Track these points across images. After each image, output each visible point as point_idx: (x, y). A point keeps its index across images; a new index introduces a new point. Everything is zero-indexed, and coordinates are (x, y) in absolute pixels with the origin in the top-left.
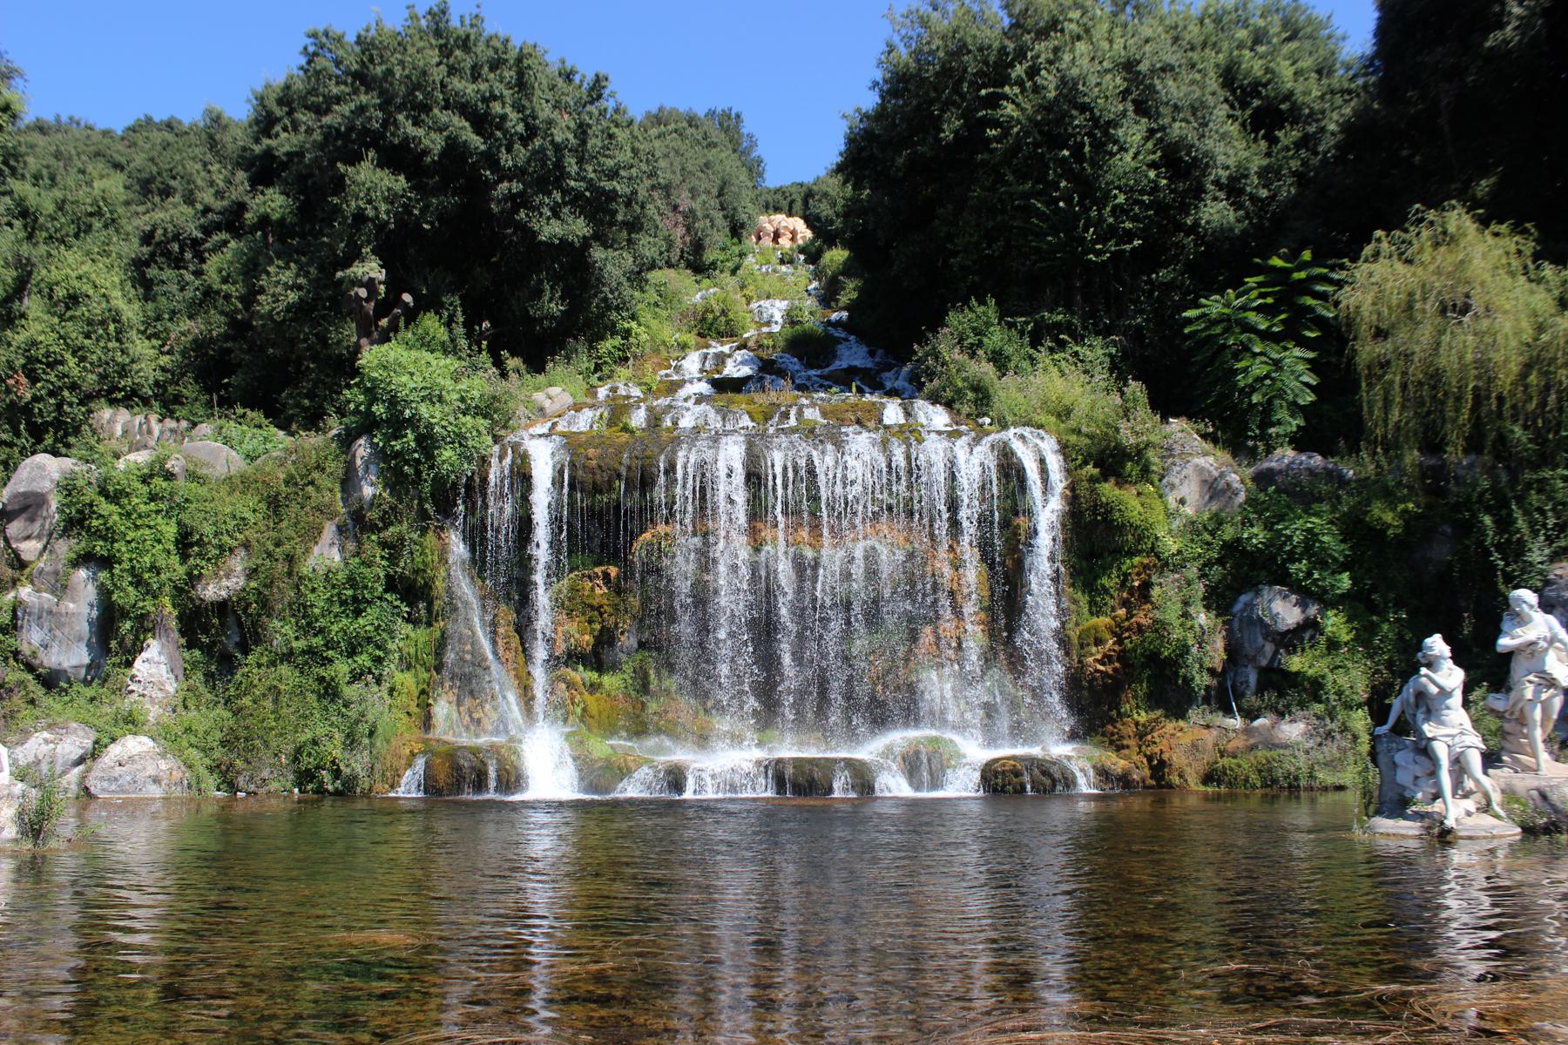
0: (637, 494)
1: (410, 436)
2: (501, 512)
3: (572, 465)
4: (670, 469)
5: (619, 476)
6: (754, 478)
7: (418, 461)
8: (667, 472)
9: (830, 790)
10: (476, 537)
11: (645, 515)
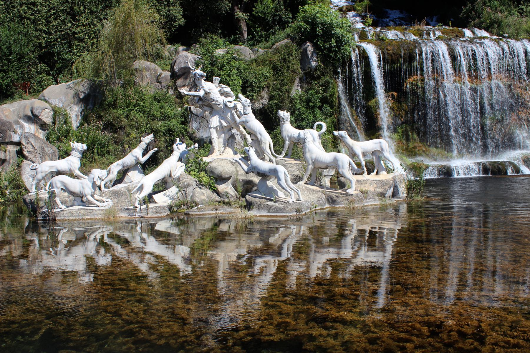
0: (407, 63)
1: (333, 41)
2: (357, 71)
3: (383, 53)
4: (421, 53)
5: (401, 57)
6: (454, 57)
7: (336, 51)
8: (419, 55)
9: (506, 173)
10: (348, 82)
11: (411, 72)
